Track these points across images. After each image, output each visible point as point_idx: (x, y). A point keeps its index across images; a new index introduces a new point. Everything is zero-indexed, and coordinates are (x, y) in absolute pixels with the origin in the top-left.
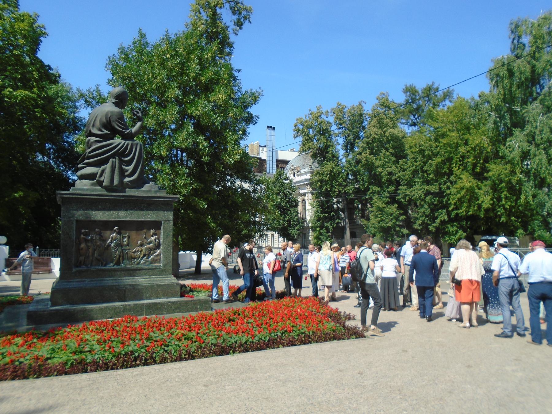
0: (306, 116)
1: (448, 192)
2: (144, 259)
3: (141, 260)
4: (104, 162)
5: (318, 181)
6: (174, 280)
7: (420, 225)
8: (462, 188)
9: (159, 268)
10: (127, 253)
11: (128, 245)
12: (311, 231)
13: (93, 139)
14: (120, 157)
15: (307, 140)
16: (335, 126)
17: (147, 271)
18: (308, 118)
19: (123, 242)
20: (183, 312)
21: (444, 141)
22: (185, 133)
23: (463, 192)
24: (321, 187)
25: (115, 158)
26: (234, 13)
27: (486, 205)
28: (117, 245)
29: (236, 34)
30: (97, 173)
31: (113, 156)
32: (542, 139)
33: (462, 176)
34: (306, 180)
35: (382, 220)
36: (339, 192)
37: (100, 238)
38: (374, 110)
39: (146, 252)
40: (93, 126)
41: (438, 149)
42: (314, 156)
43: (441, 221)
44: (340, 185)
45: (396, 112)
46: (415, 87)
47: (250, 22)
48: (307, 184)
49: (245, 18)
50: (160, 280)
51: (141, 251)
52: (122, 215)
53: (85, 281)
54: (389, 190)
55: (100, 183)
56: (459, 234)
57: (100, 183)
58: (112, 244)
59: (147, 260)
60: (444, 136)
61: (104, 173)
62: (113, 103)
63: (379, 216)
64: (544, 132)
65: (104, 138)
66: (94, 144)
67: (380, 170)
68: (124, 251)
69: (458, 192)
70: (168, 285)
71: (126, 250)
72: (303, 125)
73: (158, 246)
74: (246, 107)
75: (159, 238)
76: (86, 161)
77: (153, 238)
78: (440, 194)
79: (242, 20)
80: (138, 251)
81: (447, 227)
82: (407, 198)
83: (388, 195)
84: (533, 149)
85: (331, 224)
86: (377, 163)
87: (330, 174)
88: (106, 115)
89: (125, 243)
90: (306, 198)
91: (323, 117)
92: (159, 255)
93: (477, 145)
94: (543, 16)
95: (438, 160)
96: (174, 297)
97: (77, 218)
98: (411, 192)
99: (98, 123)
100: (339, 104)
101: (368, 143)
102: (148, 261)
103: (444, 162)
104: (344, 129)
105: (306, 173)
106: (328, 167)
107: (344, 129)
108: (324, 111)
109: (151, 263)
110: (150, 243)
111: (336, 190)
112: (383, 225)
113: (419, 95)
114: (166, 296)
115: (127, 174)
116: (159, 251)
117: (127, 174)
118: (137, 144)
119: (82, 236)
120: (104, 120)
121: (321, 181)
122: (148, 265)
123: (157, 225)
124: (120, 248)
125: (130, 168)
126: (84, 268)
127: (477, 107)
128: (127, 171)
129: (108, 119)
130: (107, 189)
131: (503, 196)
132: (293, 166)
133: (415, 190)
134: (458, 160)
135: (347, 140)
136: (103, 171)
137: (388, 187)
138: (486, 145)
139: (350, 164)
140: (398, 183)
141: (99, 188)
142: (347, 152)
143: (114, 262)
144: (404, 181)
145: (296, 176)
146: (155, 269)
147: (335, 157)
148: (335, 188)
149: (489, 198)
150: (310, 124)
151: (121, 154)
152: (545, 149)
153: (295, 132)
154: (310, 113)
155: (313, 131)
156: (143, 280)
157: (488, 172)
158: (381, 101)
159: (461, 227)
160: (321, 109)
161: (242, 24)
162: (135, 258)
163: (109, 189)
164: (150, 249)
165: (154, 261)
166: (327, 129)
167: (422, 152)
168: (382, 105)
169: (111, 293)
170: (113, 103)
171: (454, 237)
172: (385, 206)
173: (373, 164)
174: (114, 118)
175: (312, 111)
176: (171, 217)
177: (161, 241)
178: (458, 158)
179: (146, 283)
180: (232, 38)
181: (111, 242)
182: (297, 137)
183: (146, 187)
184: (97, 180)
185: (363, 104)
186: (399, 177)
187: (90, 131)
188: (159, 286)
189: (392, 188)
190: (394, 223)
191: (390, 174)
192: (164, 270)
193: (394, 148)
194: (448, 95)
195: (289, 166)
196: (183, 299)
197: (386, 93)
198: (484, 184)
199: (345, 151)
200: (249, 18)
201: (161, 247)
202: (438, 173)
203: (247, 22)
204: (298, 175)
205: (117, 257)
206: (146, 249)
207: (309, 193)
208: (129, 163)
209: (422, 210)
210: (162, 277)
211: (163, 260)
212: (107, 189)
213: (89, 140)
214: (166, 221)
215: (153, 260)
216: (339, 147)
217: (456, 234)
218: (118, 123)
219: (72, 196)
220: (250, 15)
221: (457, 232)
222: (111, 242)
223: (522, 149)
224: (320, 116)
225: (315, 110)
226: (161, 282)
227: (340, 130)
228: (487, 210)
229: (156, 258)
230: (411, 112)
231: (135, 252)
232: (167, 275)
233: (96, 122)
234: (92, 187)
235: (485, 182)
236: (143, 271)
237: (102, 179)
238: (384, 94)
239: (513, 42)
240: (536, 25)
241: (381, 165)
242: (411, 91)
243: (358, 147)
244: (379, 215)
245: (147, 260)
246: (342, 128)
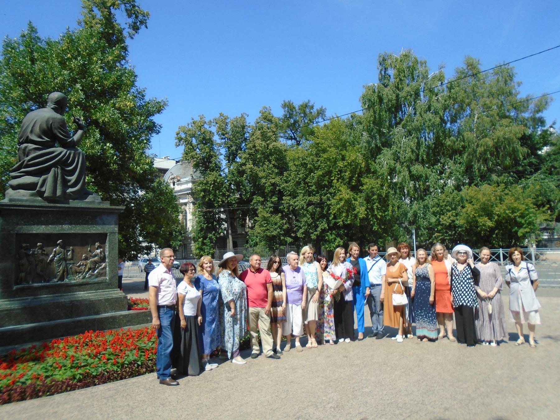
0: (188, 125)
1: (329, 202)
2: (89, 273)
3: (86, 274)
4: (46, 171)
5: (201, 191)
6: (121, 293)
7: (303, 233)
8: (341, 200)
9: (106, 282)
10: (71, 268)
11: (72, 259)
12: (193, 242)
13: (33, 146)
14: (64, 167)
15: (190, 149)
16: (217, 136)
17: (93, 285)
18: (190, 127)
19: (67, 255)
20: (134, 325)
21: (325, 156)
22: (92, 140)
23: (342, 203)
24: (204, 197)
25: (58, 168)
26: (130, 16)
27: (361, 216)
28: (60, 260)
29: (132, 38)
30: (37, 183)
31: (54, 165)
32: (405, 158)
33: (340, 188)
34: (187, 189)
35: (268, 230)
36: (223, 201)
37: (42, 252)
38: (258, 123)
39: (92, 265)
40: (32, 132)
41: (319, 163)
42: (196, 166)
43: (322, 229)
44: (224, 195)
45: (276, 125)
46: (293, 103)
47: (147, 27)
48: (188, 194)
49: (142, 23)
50: (107, 294)
51: (86, 265)
52: (66, 229)
54: (273, 200)
55: (41, 194)
56: (337, 241)
57: (41, 194)
58: (55, 258)
59: (93, 273)
60: (324, 151)
61: (46, 184)
62: (52, 108)
63: (265, 225)
64: (407, 152)
65: (45, 145)
66: (33, 152)
67: (263, 181)
68: (68, 265)
69: (338, 203)
70: (115, 298)
71: (70, 264)
72: (185, 133)
73: (103, 260)
74: (150, 114)
75: (104, 251)
77: (98, 251)
78: (321, 204)
79: (138, 24)
80: (83, 265)
81: (327, 236)
82: (291, 208)
83: (272, 205)
84: (398, 166)
85: (214, 235)
86: (261, 174)
87: (214, 184)
88: (47, 121)
89: (70, 257)
90: (187, 208)
91: (206, 126)
92: (105, 268)
93: (353, 161)
94: (404, 53)
95: (320, 173)
96: (122, 310)
97: (17, 231)
98: (295, 203)
99: (37, 130)
100: (221, 115)
101: (250, 154)
103: (324, 175)
104: (226, 139)
105: (187, 182)
106: (211, 178)
107: (226, 139)
108: (207, 120)
110: (95, 256)
111: (220, 200)
112: (268, 234)
113: (296, 110)
114: (114, 309)
115: (69, 184)
116: (104, 265)
117: (69, 184)
118: (79, 154)
119: (23, 251)
120: (45, 126)
121: (204, 190)
122: (94, 279)
123: (102, 238)
124: (64, 263)
125: (73, 178)
126: (24, 285)
127: (351, 127)
128: (70, 181)
129: (49, 126)
131: (375, 207)
132: (172, 174)
133: (298, 201)
134: (336, 173)
135: (229, 151)
136: (44, 181)
137: (271, 198)
138: (361, 161)
139: (233, 174)
140: (281, 195)
141: (40, 198)
142: (229, 162)
143: (58, 277)
144: (287, 192)
145: (176, 185)
146: (100, 283)
147: (218, 168)
148: (219, 198)
149: (364, 208)
150: (194, 133)
151: (63, 163)
153: (177, 141)
154: (192, 121)
155: (196, 140)
156: (90, 294)
157: (362, 185)
158: (265, 115)
159: (338, 235)
160: (204, 119)
161: (138, 29)
162: (79, 273)
163: (52, 199)
164: (95, 263)
165: (100, 275)
166: (210, 139)
167: (304, 165)
168: (265, 119)
169: (58, 310)
170: (52, 108)
171: (333, 245)
172: (269, 215)
173: (257, 174)
174: (56, 125)
175: (195, 119)
176: (117, 229)
177: (107, 254)
178: (336, 172)
179: (93, 297)
180: (128, 42)
181: (55, 256)
182: (179, 145)
183: (89, 199)
184: (38, 190)
185: (246, 117)
186: (283, 188)
187: (28, 137)
188: (107, 300)
189: (275, 199)
190: (279, 232)
191: (274, 185)
192: (111, 284)
193: (277, 160)
194: (321, 113)
195: (168, 174)
196: (131, 312)
197: (268, 108)
198: (359, 196)
199: (227, 162)
200: (145, 23)
201: (107, 260)
202: (320, 186)
203: (143, 27)
204: (178, 185)
205: (61, 272)
206: (92, 262)
207: (191, 203)
208: (72, 173)
209: (305, 219)
210: (108, 291)
211: (109, 274)
213: (26, 147)
214: (111, 233)
215: (99, 274)
216: (222, 157)
217: (334, 241)
218: (60, 131)
220: (146, 20)
221: (335, 239)
222: (55, 256)
223: (390, 165)
224: (203, 126)
225: (197, 119)
226: (108, 296)
227: (223, 141)
228: (362, 220)
229: (102, 272)
230: (288, 126)
231: (79, 266)
232: (114, 288)
233: (35, 127)
235: (360, 194)
236: (89, 286)
237: (43, 189)
238: (266, 108)
239: (381, 73)
240: (399, 60)
241: (264, 176)
242: (289, 107)
243: (240, 158)
244: (265, 224)
245: (93, 273)
246: (225, 138)
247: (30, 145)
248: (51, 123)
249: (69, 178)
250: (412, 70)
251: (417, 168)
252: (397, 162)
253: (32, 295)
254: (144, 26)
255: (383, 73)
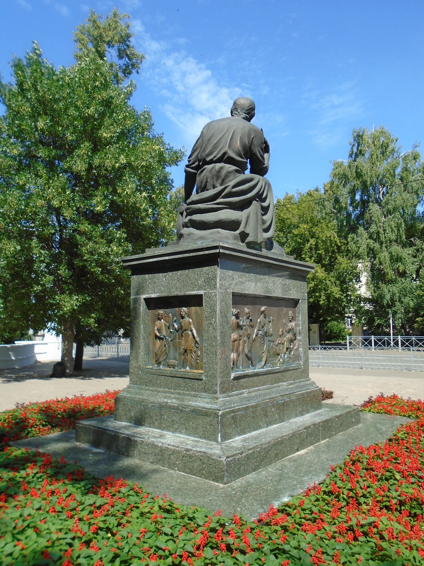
40: (230, 146)
53: (243, 393)
55: (243, 236)
57: (243, 236)
64: (387, 232)
76: (220, 200)
77: (293, 324)
84: (377, 246)
88: (249, 134)
99: (238, 144)
102: (290, 358)
109: (294, 361)
130: (250, 245)
152: (386, 247)
156: (292, 386)
164: (291, 341)
170: (244, 118)
181: (259, 330)
201: (298, 338)
212: (250, 245)
213: (221, 168)
219: (233, 253)
229: (296, 354)
234: (235, 242)
245: (291, 356)
247: (227, 166)
248: (252, 137)
249: (265, 217)
250: (384, 147)
251: (396, 249)
252: (376, 241)
253: (247, 388)
254: (135, 70)
255: (355, 150)
